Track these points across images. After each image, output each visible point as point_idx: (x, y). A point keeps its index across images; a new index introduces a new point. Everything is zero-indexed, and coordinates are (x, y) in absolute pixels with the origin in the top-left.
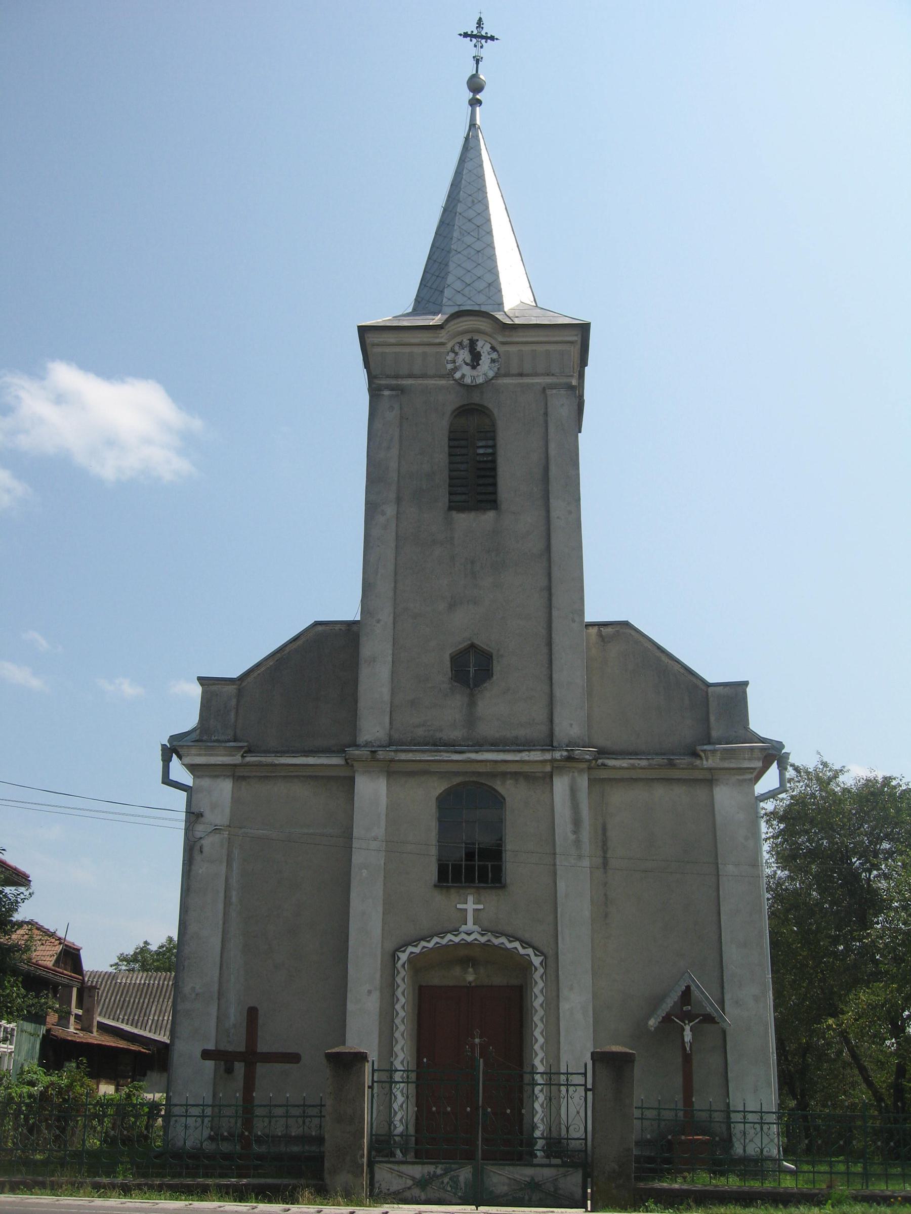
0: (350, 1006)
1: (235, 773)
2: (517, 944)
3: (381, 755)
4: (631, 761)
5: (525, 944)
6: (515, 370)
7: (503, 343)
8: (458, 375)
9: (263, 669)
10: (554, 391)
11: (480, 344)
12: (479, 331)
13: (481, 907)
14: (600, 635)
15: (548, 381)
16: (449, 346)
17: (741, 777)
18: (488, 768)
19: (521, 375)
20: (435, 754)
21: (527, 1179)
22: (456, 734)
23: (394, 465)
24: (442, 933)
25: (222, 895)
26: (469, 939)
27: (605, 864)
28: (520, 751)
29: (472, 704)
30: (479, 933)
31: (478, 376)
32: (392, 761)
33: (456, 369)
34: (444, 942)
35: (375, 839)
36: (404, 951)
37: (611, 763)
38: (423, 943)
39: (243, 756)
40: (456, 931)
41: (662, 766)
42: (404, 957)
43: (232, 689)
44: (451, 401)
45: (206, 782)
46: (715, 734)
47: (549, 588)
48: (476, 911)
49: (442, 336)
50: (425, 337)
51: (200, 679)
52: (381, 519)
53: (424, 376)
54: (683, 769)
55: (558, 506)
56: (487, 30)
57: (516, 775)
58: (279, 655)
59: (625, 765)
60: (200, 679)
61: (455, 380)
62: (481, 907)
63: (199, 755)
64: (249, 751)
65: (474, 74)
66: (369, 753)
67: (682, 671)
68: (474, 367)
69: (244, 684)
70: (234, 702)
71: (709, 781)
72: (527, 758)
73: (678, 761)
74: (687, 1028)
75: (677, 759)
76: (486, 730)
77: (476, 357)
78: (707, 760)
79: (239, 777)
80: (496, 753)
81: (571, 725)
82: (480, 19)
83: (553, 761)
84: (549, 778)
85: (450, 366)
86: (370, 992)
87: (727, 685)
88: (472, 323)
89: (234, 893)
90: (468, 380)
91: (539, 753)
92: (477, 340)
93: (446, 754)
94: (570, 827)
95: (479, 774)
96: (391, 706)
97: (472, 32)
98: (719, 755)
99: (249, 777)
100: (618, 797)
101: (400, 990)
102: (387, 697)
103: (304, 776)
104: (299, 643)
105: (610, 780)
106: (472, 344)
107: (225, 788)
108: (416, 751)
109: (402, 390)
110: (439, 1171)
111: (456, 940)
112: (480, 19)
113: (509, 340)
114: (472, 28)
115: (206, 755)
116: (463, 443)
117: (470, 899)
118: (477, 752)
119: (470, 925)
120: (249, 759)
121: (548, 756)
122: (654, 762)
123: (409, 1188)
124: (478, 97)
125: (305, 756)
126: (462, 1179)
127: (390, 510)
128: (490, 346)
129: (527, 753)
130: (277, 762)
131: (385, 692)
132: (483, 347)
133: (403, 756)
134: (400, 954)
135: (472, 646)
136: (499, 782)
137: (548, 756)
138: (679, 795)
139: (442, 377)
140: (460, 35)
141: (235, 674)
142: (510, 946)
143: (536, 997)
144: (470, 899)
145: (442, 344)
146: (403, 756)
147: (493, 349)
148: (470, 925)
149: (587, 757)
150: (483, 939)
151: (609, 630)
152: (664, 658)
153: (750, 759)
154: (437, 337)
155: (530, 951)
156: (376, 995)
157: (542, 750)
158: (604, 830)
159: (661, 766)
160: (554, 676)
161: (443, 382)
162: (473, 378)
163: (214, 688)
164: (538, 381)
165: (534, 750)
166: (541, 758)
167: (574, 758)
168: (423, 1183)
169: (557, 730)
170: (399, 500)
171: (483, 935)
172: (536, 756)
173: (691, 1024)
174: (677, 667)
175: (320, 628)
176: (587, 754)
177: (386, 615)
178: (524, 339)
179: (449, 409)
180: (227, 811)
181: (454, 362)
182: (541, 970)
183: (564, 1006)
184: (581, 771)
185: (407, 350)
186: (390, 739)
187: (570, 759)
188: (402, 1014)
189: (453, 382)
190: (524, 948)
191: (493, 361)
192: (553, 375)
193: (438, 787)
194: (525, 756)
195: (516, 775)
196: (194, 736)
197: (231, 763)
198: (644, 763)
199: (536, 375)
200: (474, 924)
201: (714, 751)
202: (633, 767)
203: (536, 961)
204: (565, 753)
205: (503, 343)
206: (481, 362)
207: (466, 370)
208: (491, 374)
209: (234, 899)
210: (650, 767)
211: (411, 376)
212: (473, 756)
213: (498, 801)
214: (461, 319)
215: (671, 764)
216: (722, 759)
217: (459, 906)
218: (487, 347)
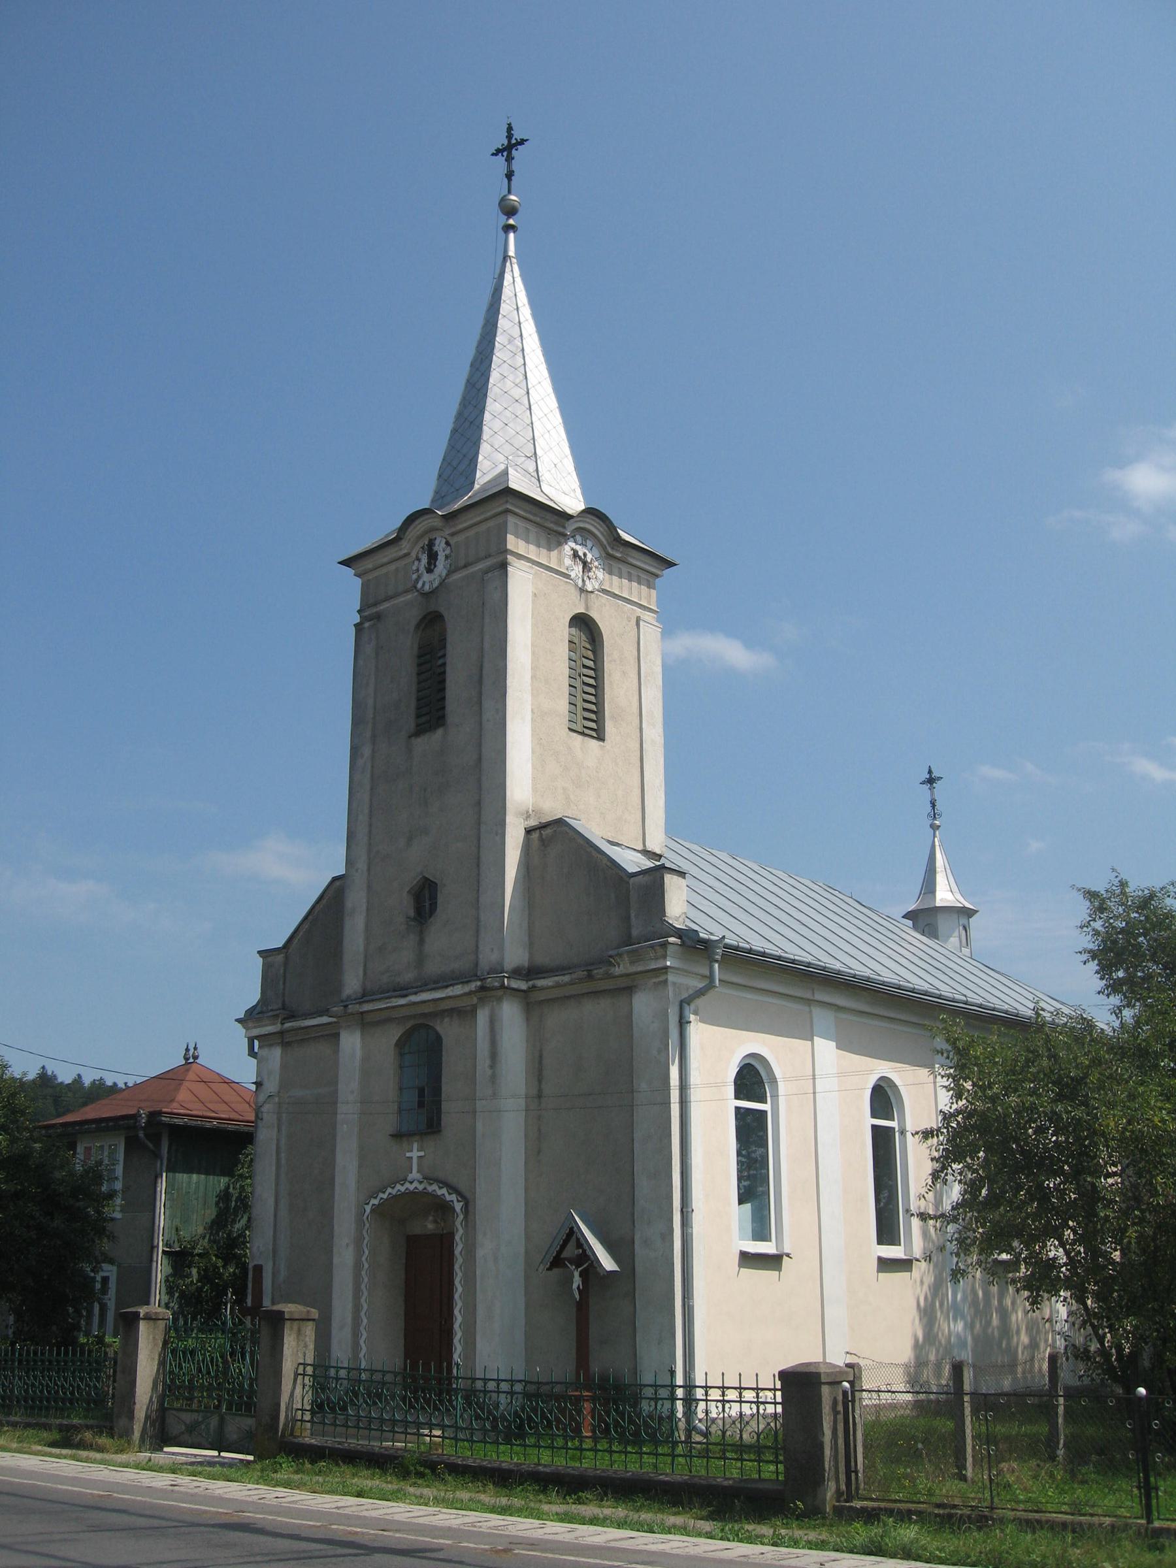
0: (336, 1260)
1: (282, 1039)
2: (444, 1191)
3: (351, 1009)
4: (556, 978)
5: (453, 1189)
6: (462, 563)
7: (453, 534)
8: (419, 585)
9: (301, 933)
10: (490, 575)
11: (437, 542)
12: (426, 532)
13: (422, 1154)
14: (541, 839)
15: (488, 564)
16: (414, 555)
17: (657, 980)
18: (426, 1009)
19: (465, 566)
20: (387, 1001)
21: (247, 1429)
22: (409, 976)
23: (370, 702)
24: (392, 1184)
25: (274, 1157)
26: (411, 1187)
27: (540, 1096)
28: (447, 987)
29: (421, 942)
30: (418, 1181)
31: (435, 579)
32: (362, 1013)
33: (417, 581)
34: (394, 1192)
35: (352, 1092)
36: (368, 1204)
37: (540, 983)
38: (381, 1195)
39: (282, 1024)
40: (405, 1180)
41: (581, 979)
42: (368, 1208)
43: (280, 958)
44: (413, 616)
45: (265, 1052)
46: (635, 932)
47: (479, 803)
48: (420, 1157)
49: (405, 546)
50: (391, 553)
51: (259, 952)
52: (360, 762)
53: (397, 595)
54: (600, 979)
55: (488, 704)
56: (518, 135)
57: (451, 1012)
58: (310, 917)
59: (550, 984)
60: (259, 952)
61: (418, 591)
62: (422, 1154)
63: (255, 1027)
64: (292, 1016)
65: (505, 196)
66: (342, 1008)
67: (609, 864)
68: (429, 570)
69: (290, 951)
70: (282, 971)
71: (627, 989)
72: (451, 994)
73: (595, 971)
74: (576, 1274)
75: (596, 969)
76: (433, 967)
77: (433, 557)
78: (619, 967)
79: (287, 1043)
80: (440, 991)
81: (492, 950)
82: (509, 125)
83: (470, 993)
84: (473, 1011)
85: (415, 576)
86: (347, 1245)
87: (646, 873)
88: (426, 522)
89: (283, 1155)
90: (427, 588)
91: (460, 986)
92: (435, 539)
93: (394, 1000)
94: (488, 1062)
95: (424, 1015)
96: (366, 957)
97: (503, 145)
98: (627, 959)
99: (292, 1042)
100: (556, 1018)
101: (365, 1242)
102: (362, 948)
103: (327, 1035)
104: (324, 901)
105: (548, 1001)
106: (431, 544)
107: (277, 1052)
108: (373, 1000)
109: (378, 617)
110: (200, 1419)
111: (403, 1189)
112: (509, 125)
113: (453, 530)
114: (518, 135)
115: (259, 1027)
116: (428, 657)
117: (415, 1146)
118: (416, 993)
119: (415, 1174)
120: (288, 1025)
121: (467, 988)
122: (574, 976)
123: (183, 1433)
124: (511, 222)
125: (319, 1016)
126: (212, 1426)
127: (367, 751)
128: (444, 540)
129: (451, 988)
130: (303, 1025)
131: (361, 941)
132: (440, 547)
133: (367, 1007)
134: (366, 1206)
135: (426, 879)
136: (438, 1022)
137: (467, 988)
138: (594, 1011)
139: (406, 591)
140: (493, 154)
141: (280, 944)
142: (440, 1192)
143: (457, 1244)
144: (415, 1146)
145: (407, 555)
146: (367, 1007)
147: (447, 543)
148: (415, 1174)
149: (496, 984)
150: (421, 1187)
151: (548, 831)
152: (594, 853)
153: (656, 959)
154: (401, 550)
155: (454, 1197)
156: (351, 1248)
157: (462, 983)
158: (541, 1056)
159: (581, 980)
160: (481, 899)
161: (409, 596)
162: (431, 582)
163: (270, 959)
164: (480, 567)
165: (457, 984)
166: (462, 992)
167: (486, 987)
168: (191, 1428)
169: (481, 956)
170: (374, 737)
171: (421, 1183)
172: (458, 990)
173: (579, 1269)
174: (605, 861)
175: (338, 883)
176: (497, 981)
177: (362, 865)
178: (465, 525)
179: (414, 622)
180: (278, 1077)
181: (418, 570)
182: (461, 1217)
183: (480, 1253)
184: (499, 999)
185: (384, 570)
186: (364, 990)
187: (483, 988)
188: (366, 1266)
189: (416, 594)
190: (450, 1194)
191: (447, 557)
192: (490, 556)
193: (394, 1033)
194: (449, 992)
195: (451, 1012)
196: (258, 1009)
197: (275, 1031)
198: (566, 978)
199: (478, 560)
200: (418, 1172)
201: (620, 955)
202: (558, 985)
203: (458, 1206)
204: (479, 983)
205: (453, 534)
206: (437, 563)
207: (426, 577)
208: (444, 574)
209: (283, 1162)
210: (571, 983)
211: (388, 598)
212: (414, 998)
213: (439, 1039)
214: (417, 522)
215: (590, 977)
216: (632, 963)
217: (408, 1155)
218: (443, 545)
